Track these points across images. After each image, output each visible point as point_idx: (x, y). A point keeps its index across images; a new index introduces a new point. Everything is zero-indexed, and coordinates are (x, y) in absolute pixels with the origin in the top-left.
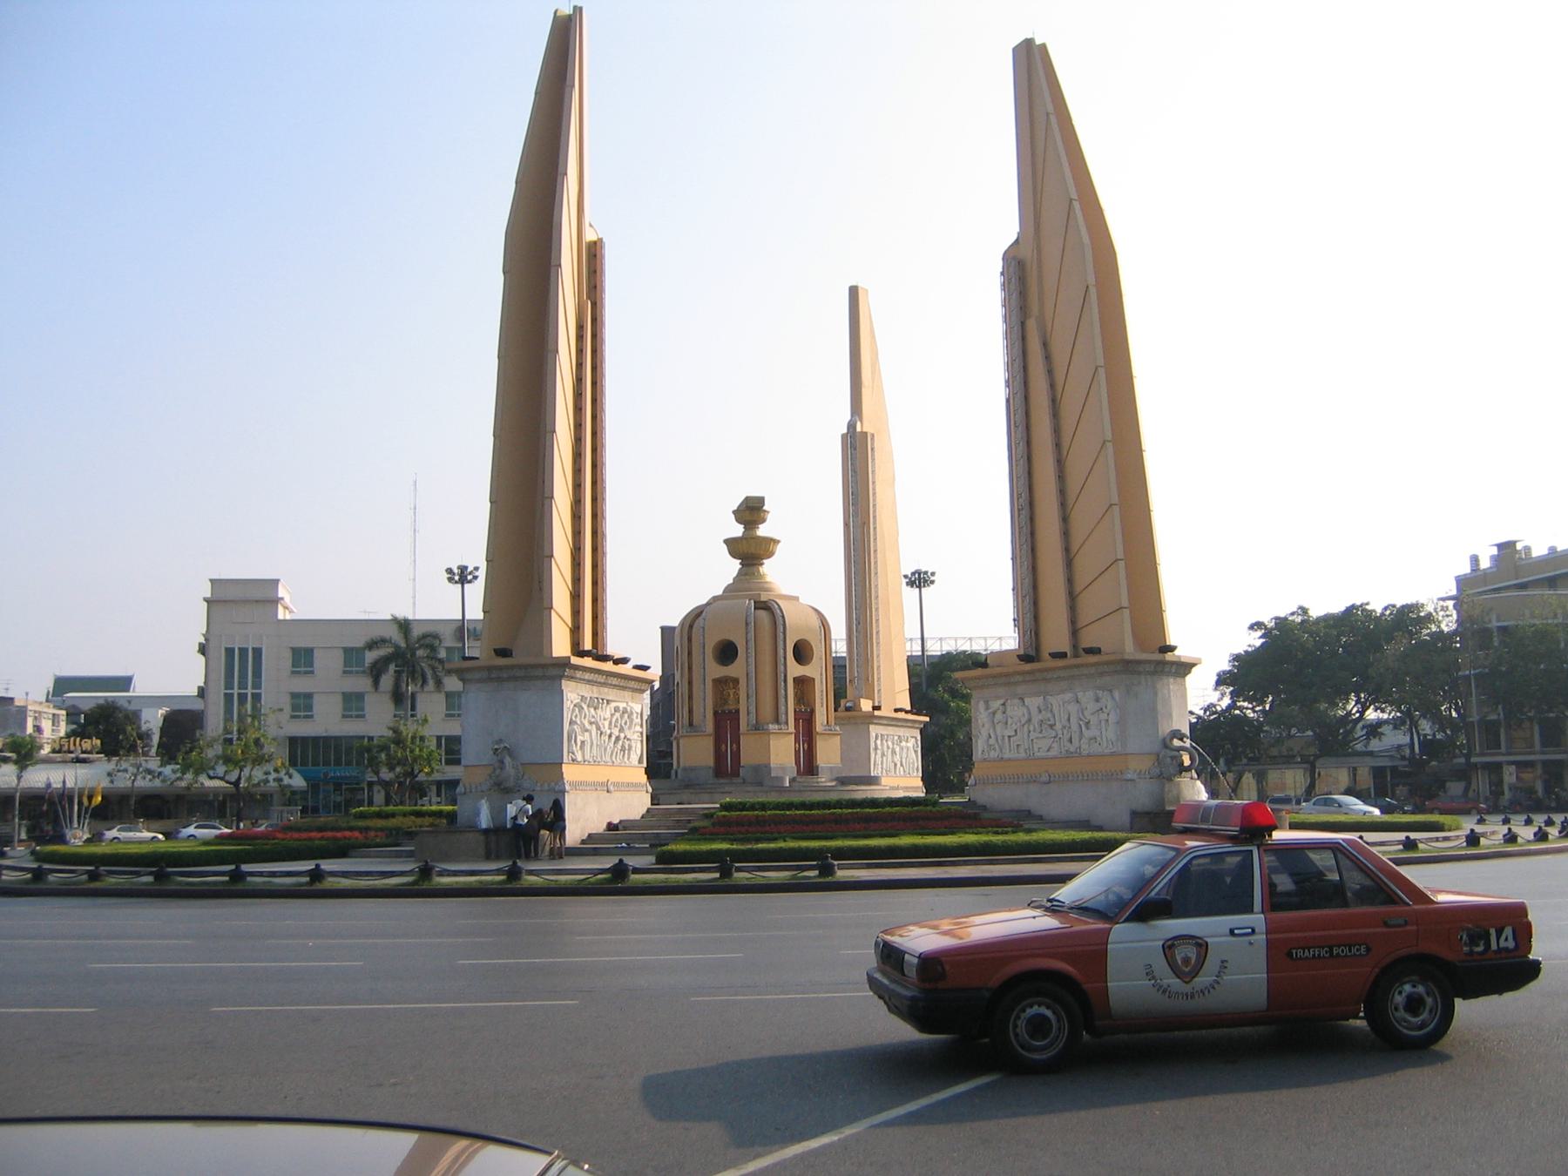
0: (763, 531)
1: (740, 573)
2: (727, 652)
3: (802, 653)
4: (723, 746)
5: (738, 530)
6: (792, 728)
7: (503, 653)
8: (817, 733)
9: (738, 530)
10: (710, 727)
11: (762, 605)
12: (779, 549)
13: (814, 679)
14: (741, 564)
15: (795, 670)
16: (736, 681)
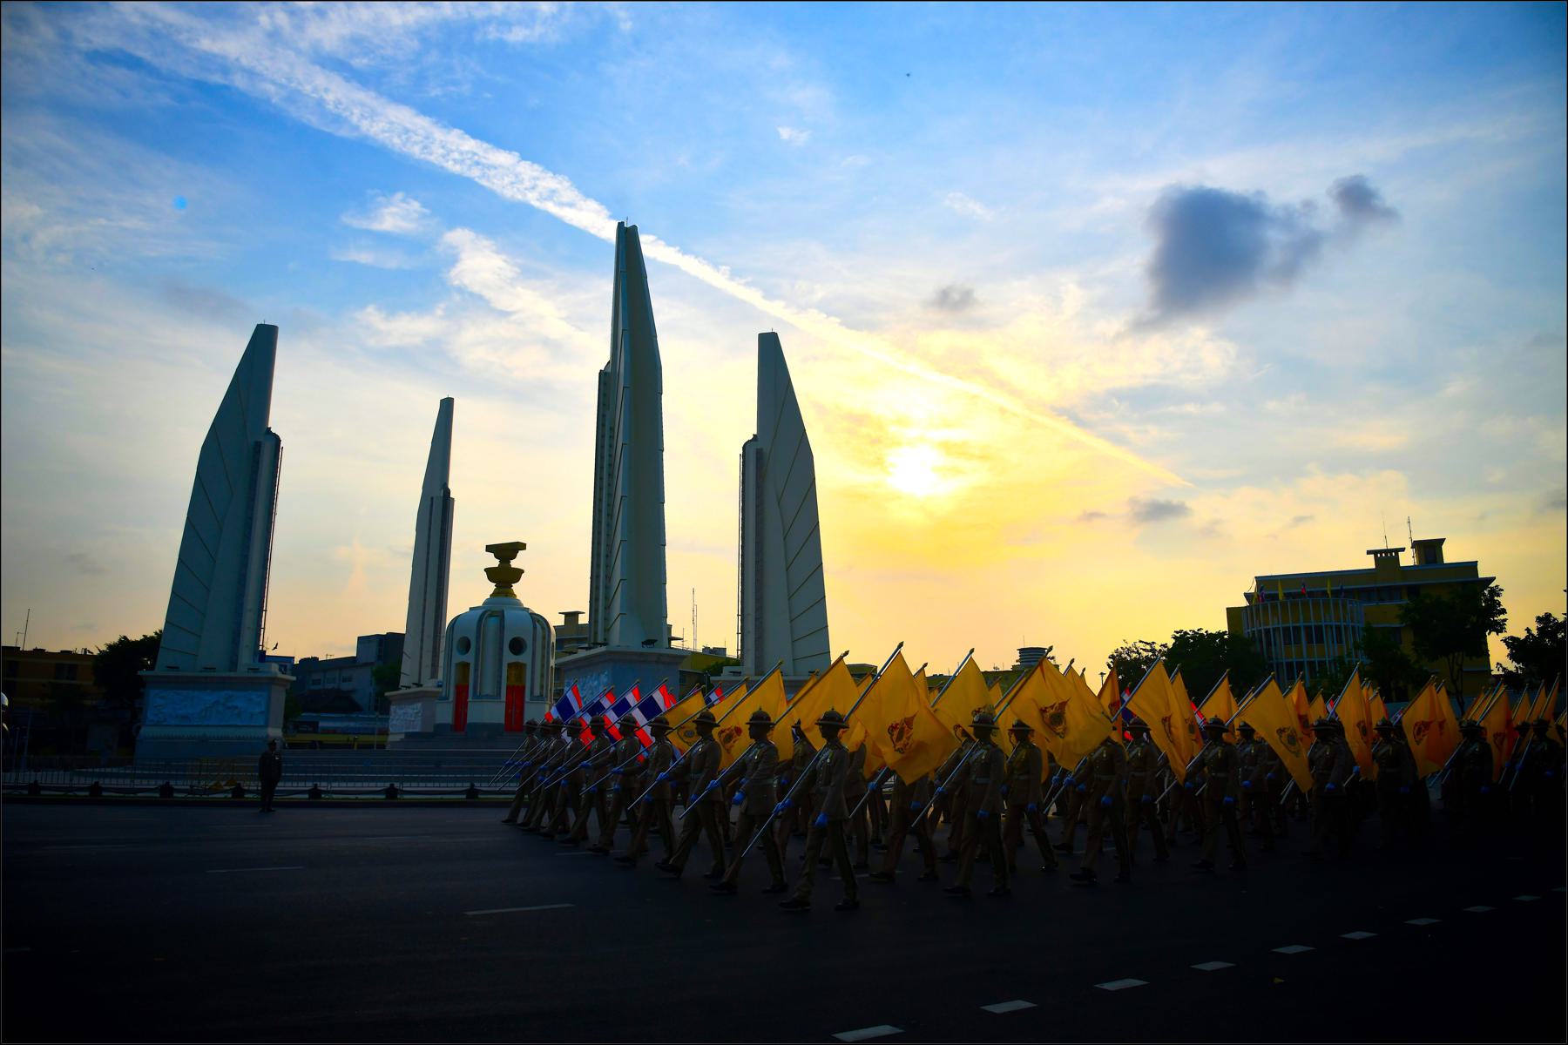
0: (514, 564)
1: (493, 595)
2: (465, 645)
3: (517, 646)
5: (495, 563)
9: (495, 563)
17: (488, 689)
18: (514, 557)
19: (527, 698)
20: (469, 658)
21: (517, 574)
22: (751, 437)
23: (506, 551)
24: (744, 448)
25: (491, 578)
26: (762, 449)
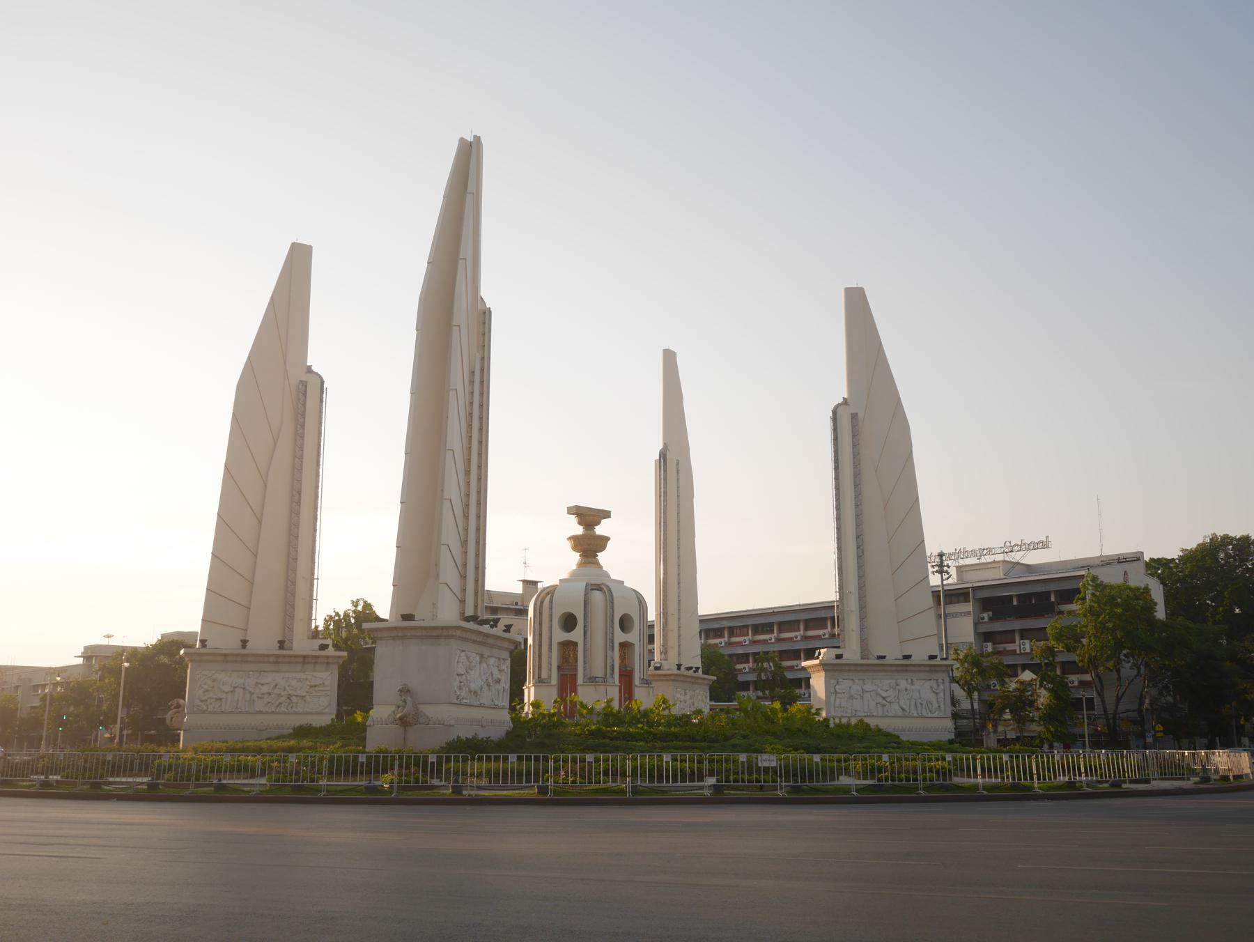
0: (600, 530)
1: (579, 565)
2: (569, 622)
4: (565, 694)
5: (579, 530)
6: (617, 682)
7: (408, 617)
8: (636, 686)
9: (579, 530)
10: (554, 681)
11: (597, 587)
12: (609, 544)
13: (634, 644)
14: (580, 556)
15: (620, 637)
16: (575, 644)
17: (598, 672)
18: (598, 523)
19: (637, 681)
20: (576, 635)
21: (604, 540)
22: (841, 401)
23: (589, 517)
24: (834, 412)
25: (575, 548)
26: (857, 414)
